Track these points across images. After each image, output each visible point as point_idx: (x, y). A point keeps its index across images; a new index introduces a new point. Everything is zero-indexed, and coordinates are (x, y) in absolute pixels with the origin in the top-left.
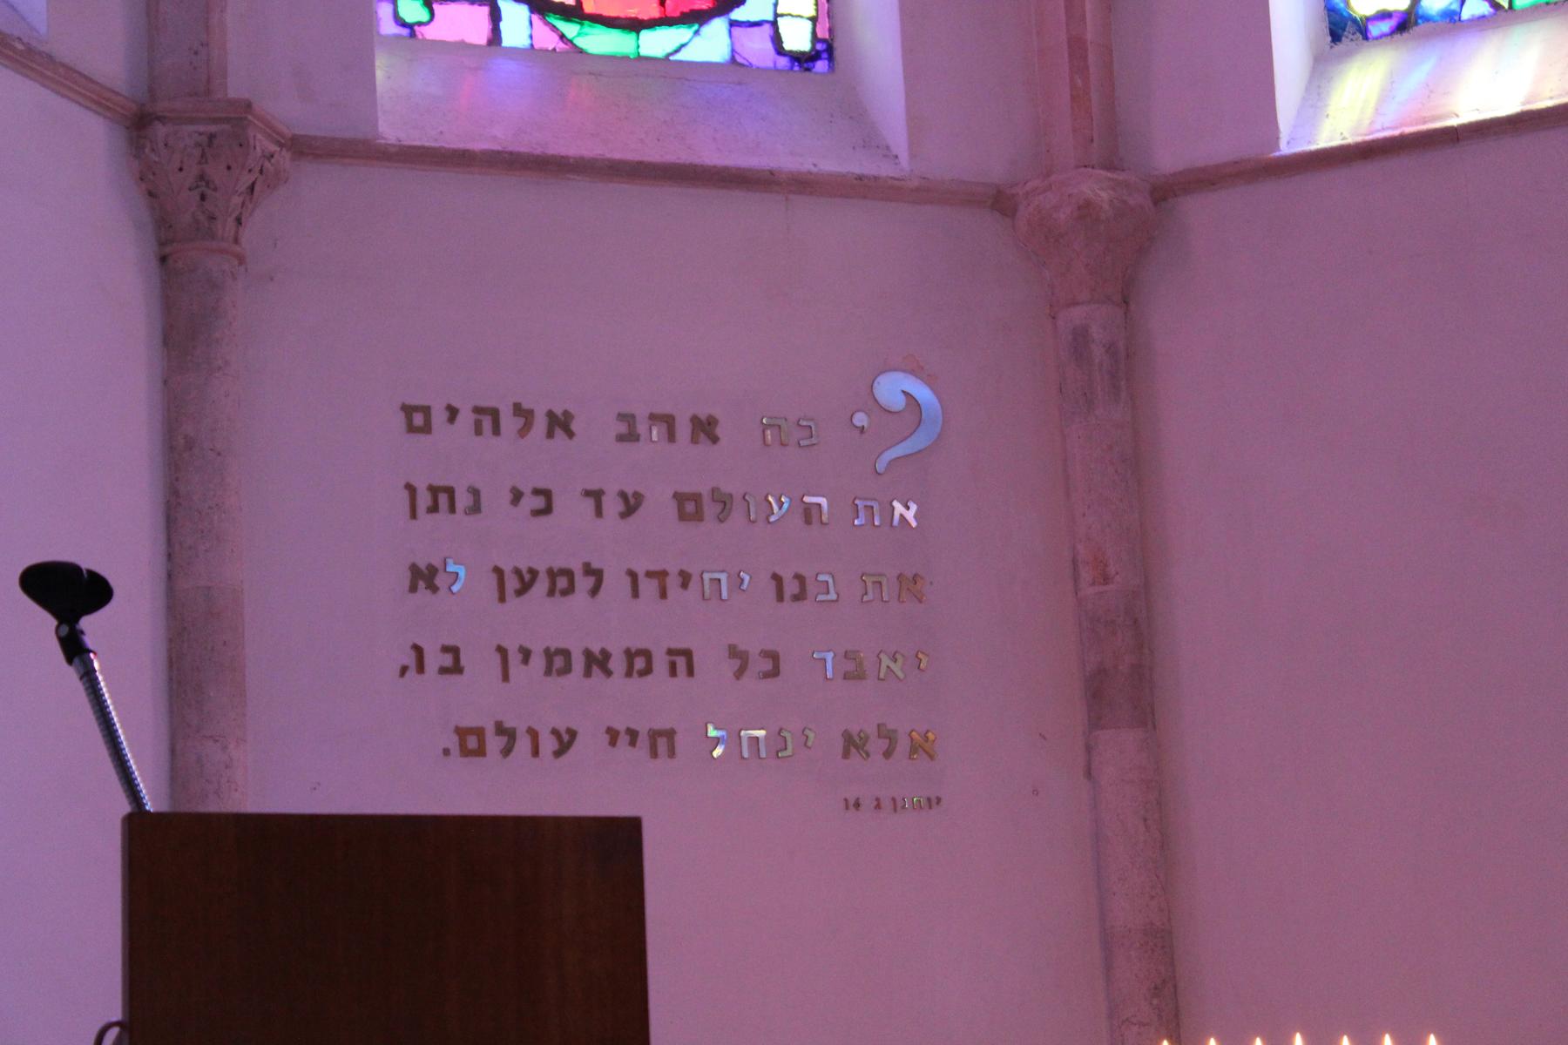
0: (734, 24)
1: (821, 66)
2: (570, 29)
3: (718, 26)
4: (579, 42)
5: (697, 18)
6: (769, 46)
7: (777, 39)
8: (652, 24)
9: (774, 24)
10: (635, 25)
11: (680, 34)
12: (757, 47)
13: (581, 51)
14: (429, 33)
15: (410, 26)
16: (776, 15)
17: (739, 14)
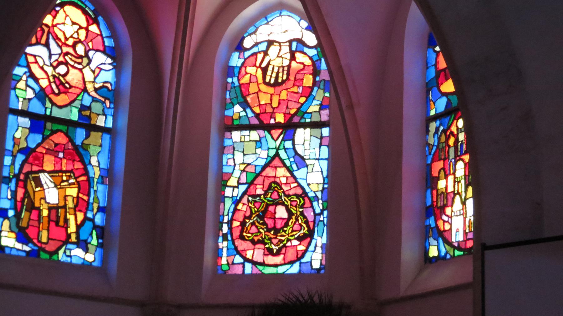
0: (301, 263)
1: (322, 272)
2: (261, 268)
3: (297, 264)
4: (263, 271)
5: (292, 263)
6: (310, 267)
7: (311, 266)
8: (281, 265)
9: (311, 262)
10: (276, 266)
11: (288, 266)
12: (306, 269)
13: (263, 273)
14: (230, 272)
15: (225, 272)
16: (311, 260)
17: (303, 260)
